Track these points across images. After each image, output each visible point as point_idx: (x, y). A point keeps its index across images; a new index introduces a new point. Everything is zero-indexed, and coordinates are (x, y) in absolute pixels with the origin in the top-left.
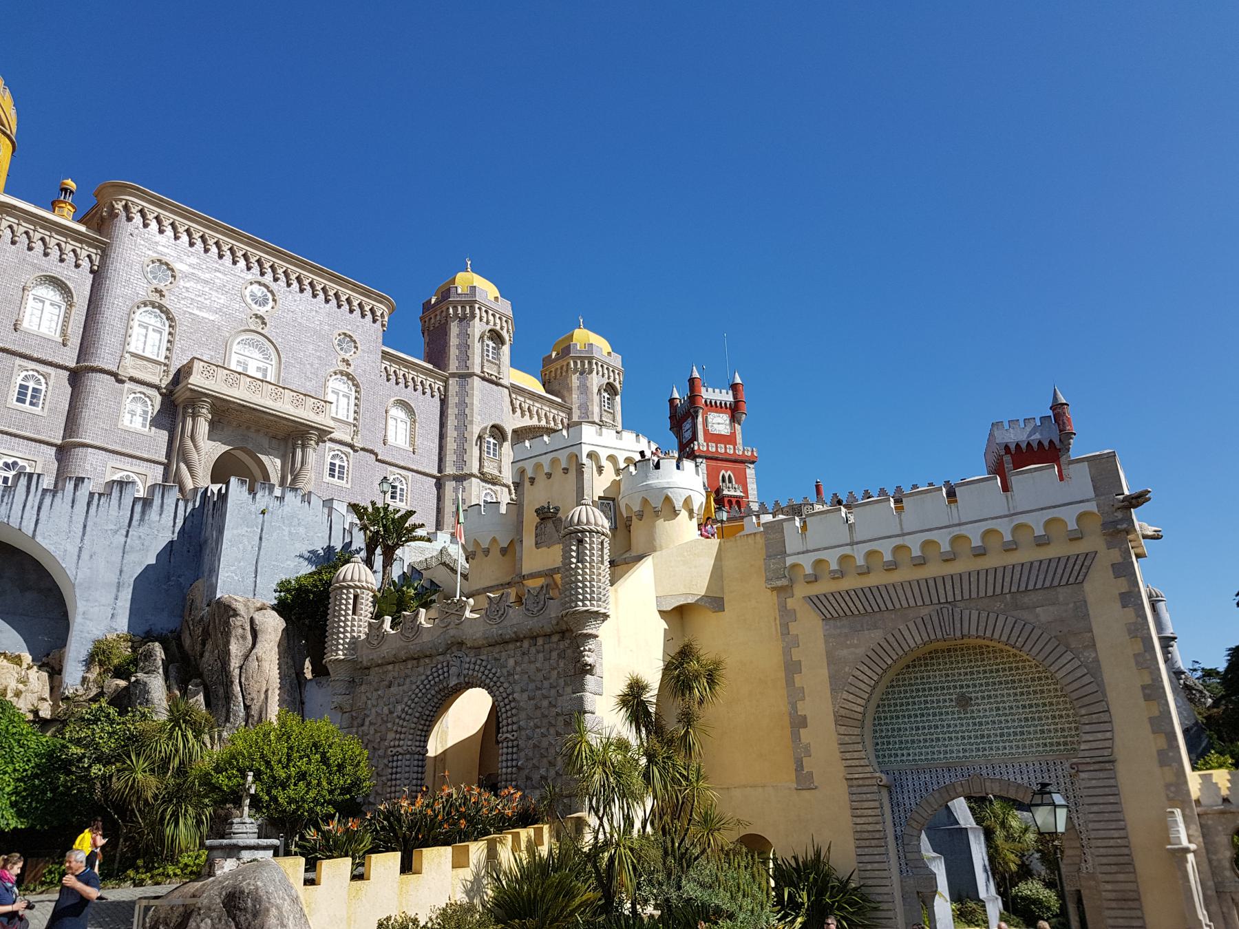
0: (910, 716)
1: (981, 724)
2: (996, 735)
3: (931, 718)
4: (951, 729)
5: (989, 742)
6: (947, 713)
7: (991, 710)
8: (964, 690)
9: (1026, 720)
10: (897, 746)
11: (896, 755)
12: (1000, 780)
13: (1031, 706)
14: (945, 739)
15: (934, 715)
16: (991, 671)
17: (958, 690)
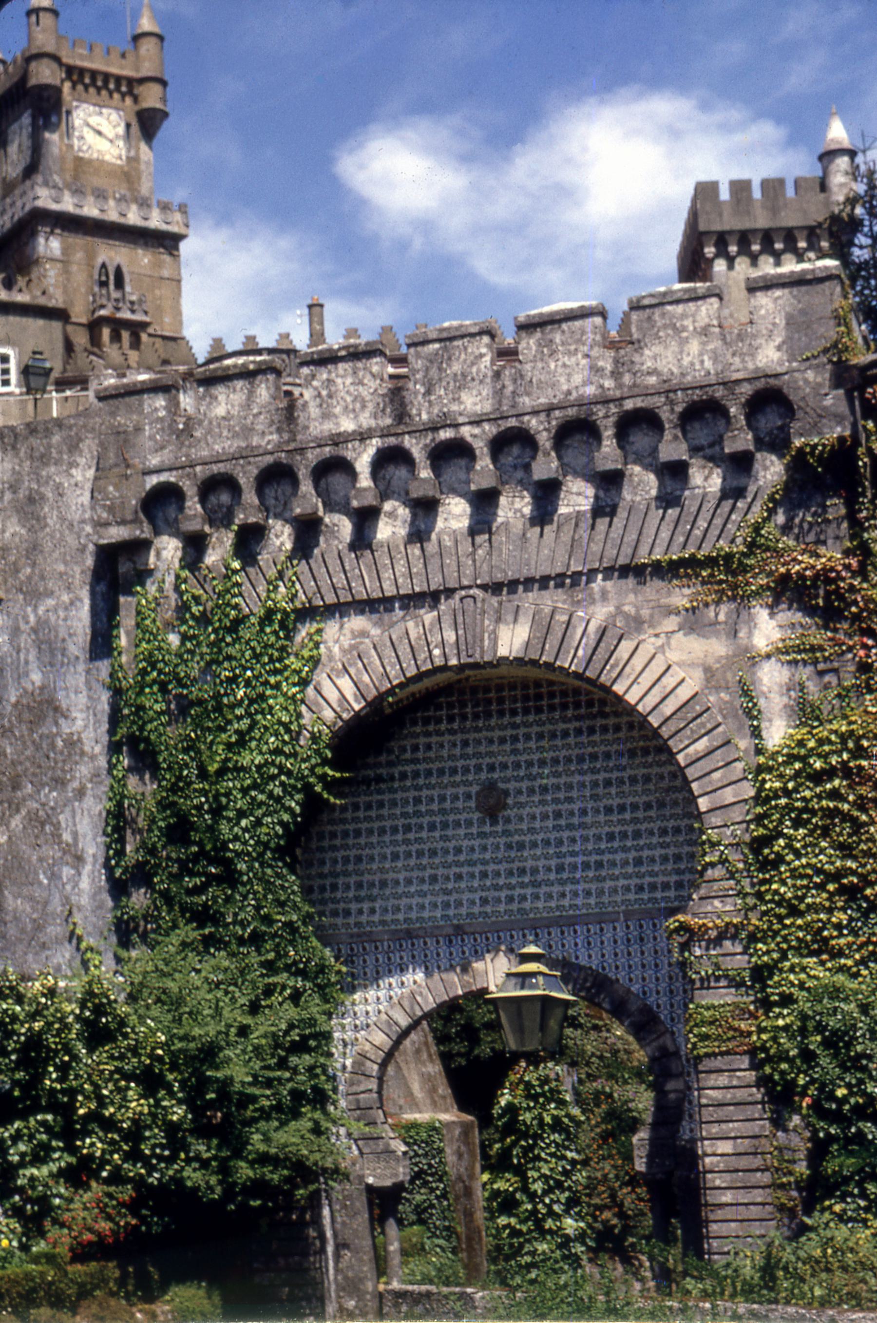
0: (382, 831)
1: (521, 846)
2: (549, 869)
3: (424, 834)
4: (462, 858)
5: (535, 884)
6: (457, 824)
7: (545, 817)
8: (496, 776)
9: (611, 837)
10: (351, 894)
13: (622, 808)
14: (448, 879)
15: (432, 827)
16: (553, 736)
17: (483, 776)
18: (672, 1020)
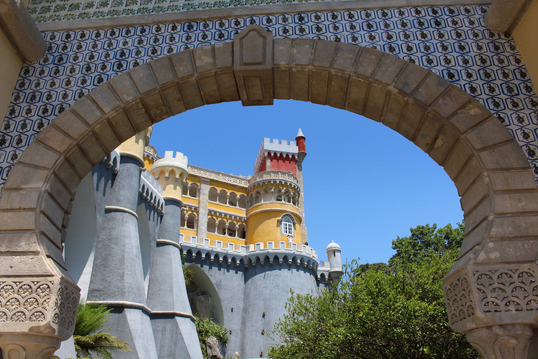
12: (314, 43)
18: (497, 105)
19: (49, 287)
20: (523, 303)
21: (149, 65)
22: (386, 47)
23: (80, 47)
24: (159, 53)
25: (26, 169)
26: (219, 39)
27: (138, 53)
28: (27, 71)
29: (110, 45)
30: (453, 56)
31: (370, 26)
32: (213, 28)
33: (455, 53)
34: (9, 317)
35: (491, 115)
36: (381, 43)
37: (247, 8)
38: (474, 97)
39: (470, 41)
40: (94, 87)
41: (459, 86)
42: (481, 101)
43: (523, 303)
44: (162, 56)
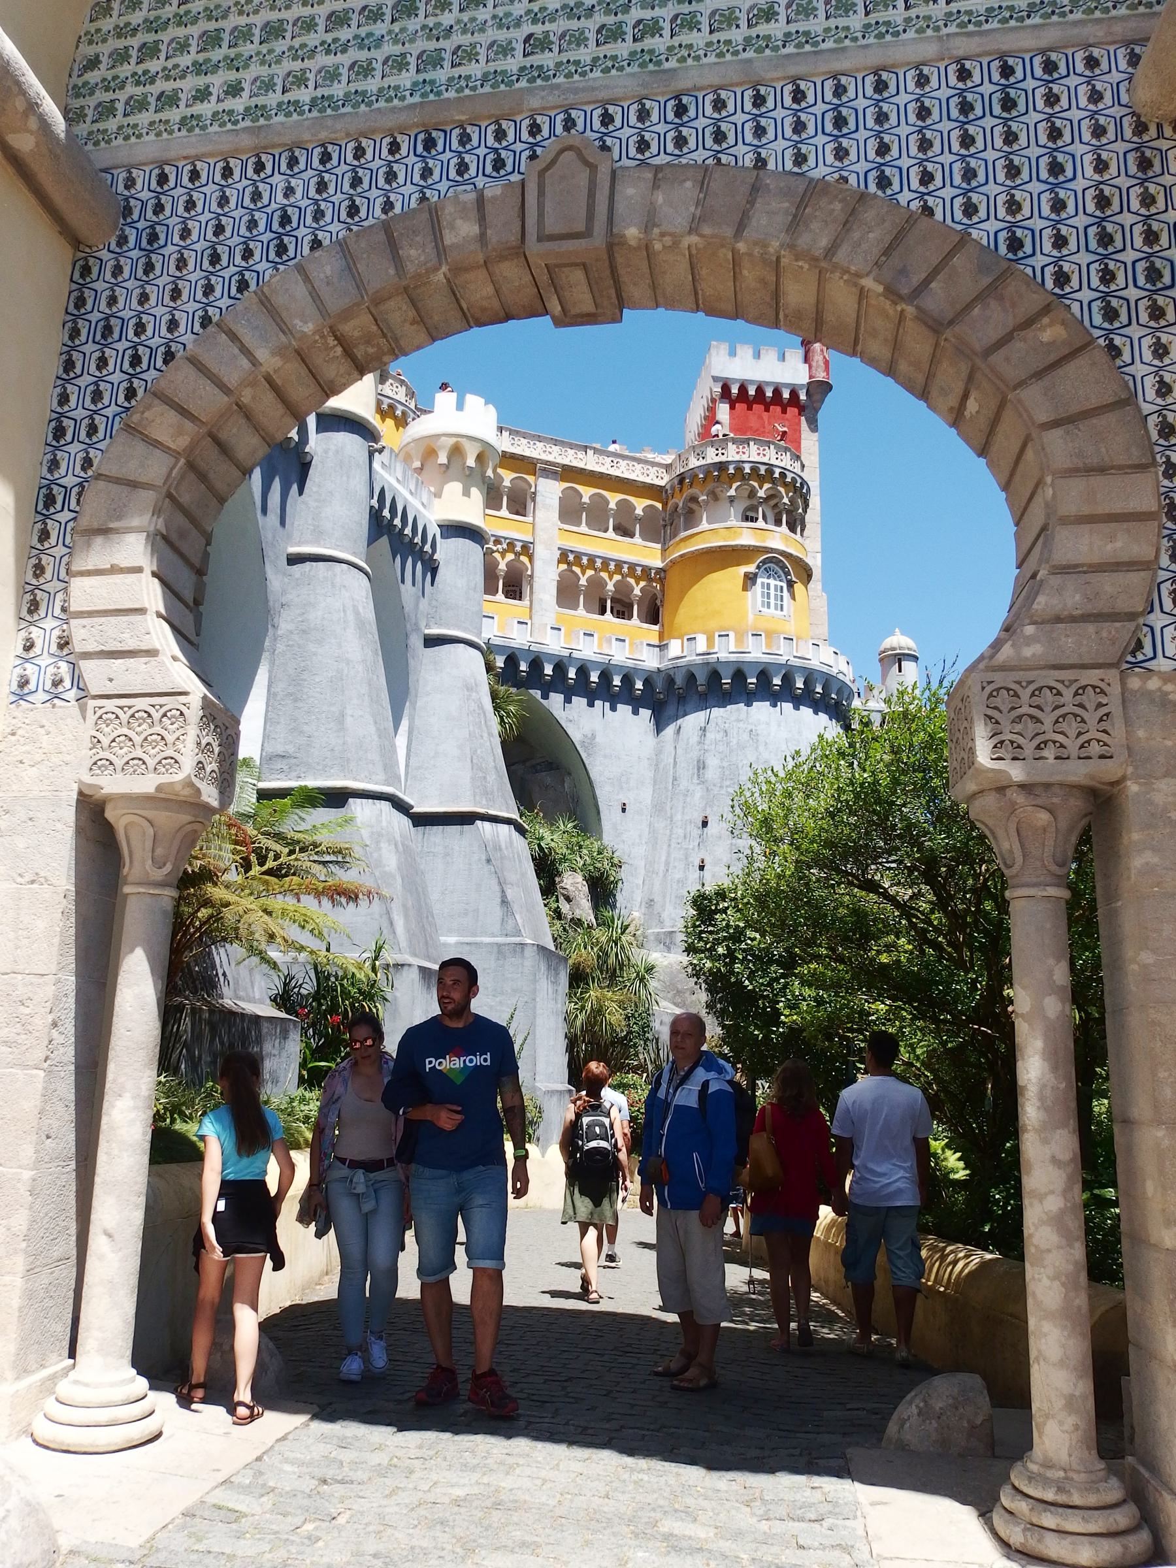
11: (169, 100)
18: (1110, 314)
19: (182, 714)
20: (1073, 746)
21: (342, 246)
22: (872, 175)
23: (190, 205)
24: (363, 214)
25: (114, 488)
26: (494, 174)
27: (319, 215)
28: (86, 270)
29: (256, 196)
30: (1032, 190)
31: (840, 122)
32: (483, 142)
33: (1038, 184)
34: (119, 769)
35: (1093, 340)
36: (862, 167)
37: (558, 86)
38: (1062, 296)
39: (1078, 149)
40: (232, 302)
41: (1029, 271)
42: (1075, 307)
43: (1073, 746)
44: (371, 221)
